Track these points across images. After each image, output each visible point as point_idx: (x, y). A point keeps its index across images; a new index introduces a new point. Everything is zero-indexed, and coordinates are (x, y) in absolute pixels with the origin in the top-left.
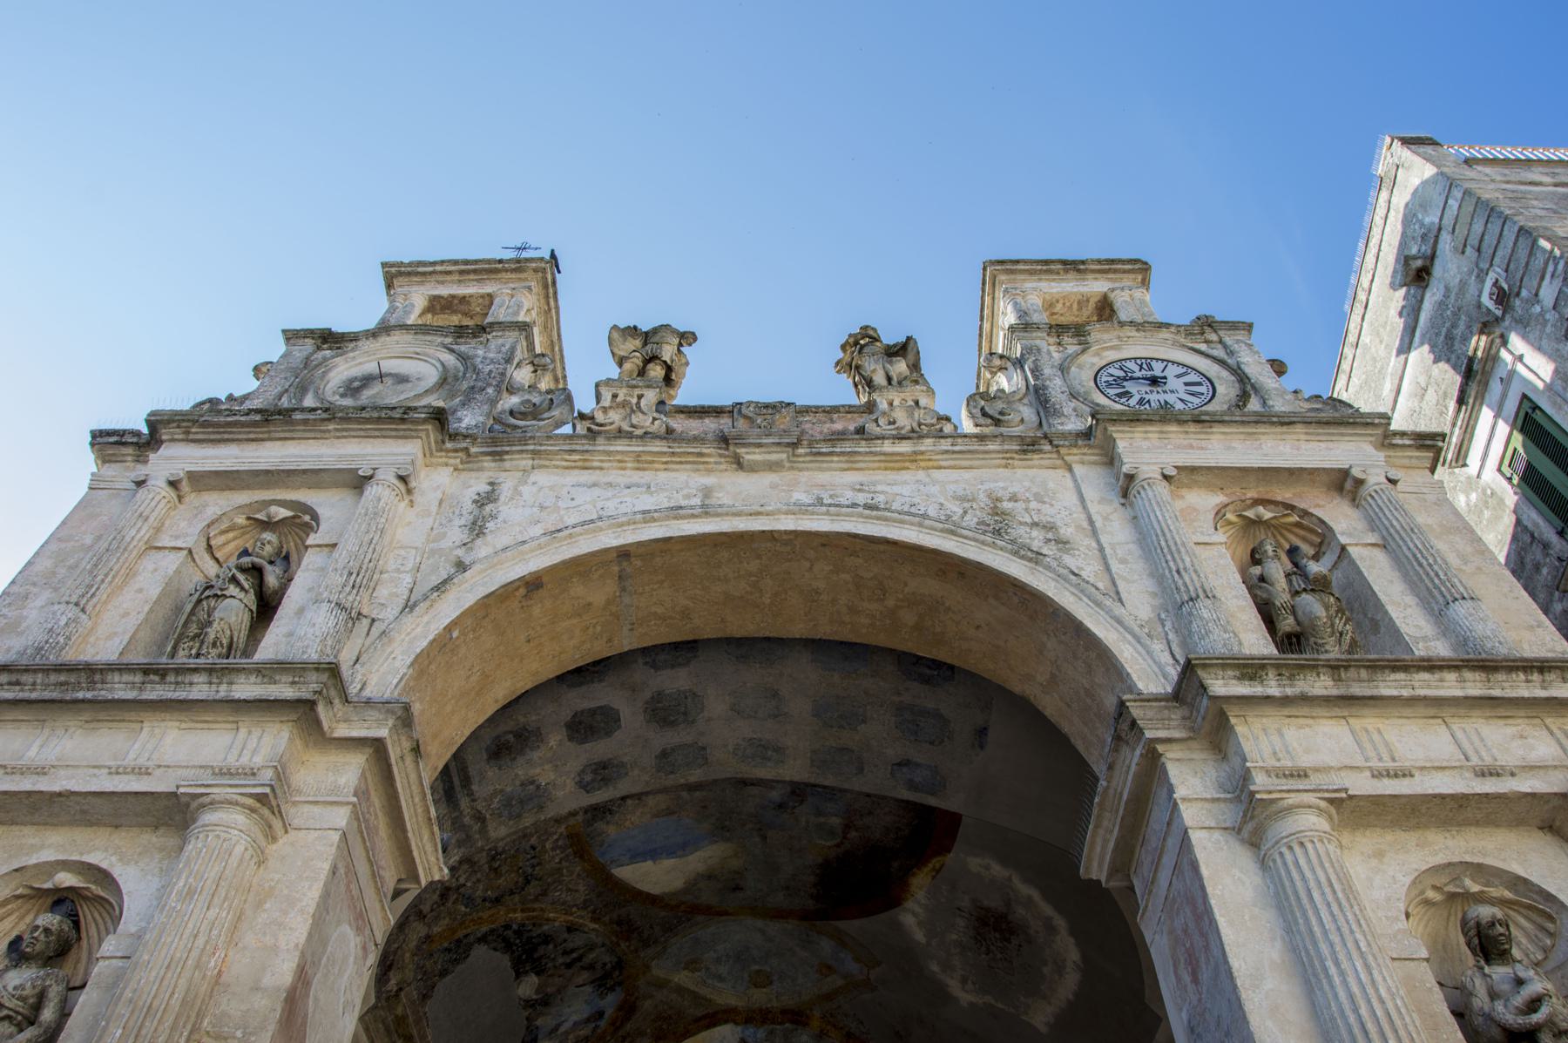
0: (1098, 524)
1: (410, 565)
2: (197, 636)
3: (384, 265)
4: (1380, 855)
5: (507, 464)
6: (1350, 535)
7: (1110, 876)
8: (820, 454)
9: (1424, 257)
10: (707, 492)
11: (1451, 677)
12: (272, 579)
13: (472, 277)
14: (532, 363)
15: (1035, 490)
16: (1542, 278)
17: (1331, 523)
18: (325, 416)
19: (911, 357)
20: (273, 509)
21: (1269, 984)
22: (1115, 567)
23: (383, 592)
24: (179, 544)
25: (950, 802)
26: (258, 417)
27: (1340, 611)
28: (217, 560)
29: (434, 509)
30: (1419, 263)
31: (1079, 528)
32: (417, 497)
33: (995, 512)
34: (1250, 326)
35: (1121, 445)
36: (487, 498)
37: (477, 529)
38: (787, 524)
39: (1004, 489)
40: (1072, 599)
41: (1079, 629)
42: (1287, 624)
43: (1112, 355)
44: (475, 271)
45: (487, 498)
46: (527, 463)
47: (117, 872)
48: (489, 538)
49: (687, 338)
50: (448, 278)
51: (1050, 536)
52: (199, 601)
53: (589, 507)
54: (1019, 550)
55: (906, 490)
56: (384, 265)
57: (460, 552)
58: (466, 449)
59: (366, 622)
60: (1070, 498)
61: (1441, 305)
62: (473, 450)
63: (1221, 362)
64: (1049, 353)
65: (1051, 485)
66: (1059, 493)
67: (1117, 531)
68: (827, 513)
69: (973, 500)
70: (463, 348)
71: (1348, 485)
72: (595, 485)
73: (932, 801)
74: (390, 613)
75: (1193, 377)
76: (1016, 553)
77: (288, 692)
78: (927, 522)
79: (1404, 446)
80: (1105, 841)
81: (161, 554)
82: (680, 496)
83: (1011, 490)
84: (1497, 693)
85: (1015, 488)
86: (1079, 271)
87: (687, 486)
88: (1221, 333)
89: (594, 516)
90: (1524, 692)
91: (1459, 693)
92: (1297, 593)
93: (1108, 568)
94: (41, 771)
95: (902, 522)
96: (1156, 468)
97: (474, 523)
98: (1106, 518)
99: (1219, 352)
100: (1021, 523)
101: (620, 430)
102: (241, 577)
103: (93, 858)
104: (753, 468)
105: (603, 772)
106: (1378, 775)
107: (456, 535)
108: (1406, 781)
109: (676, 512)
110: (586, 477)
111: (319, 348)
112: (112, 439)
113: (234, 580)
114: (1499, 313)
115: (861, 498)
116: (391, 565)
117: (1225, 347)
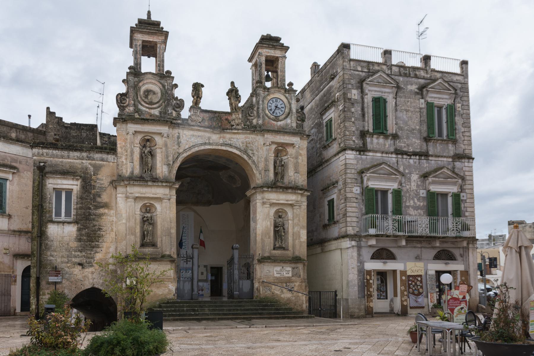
10: (209, 138)
30: (332, 77)
35: (266, 135)
36: (179, 137)
37: (179, 144)
43: (272, 96)
49: (203, 86)
54: (248, 156)
55: (235, 140)
63: (289, 102)
70: (162, 81)
72: (193, 136)
74: (171, 163)
75: (283, 106)
99: (289, 97)
103: (151, 202)
104: (215, 133)
109: (205, 144)
110: (191, 133)
115: (229, 142)
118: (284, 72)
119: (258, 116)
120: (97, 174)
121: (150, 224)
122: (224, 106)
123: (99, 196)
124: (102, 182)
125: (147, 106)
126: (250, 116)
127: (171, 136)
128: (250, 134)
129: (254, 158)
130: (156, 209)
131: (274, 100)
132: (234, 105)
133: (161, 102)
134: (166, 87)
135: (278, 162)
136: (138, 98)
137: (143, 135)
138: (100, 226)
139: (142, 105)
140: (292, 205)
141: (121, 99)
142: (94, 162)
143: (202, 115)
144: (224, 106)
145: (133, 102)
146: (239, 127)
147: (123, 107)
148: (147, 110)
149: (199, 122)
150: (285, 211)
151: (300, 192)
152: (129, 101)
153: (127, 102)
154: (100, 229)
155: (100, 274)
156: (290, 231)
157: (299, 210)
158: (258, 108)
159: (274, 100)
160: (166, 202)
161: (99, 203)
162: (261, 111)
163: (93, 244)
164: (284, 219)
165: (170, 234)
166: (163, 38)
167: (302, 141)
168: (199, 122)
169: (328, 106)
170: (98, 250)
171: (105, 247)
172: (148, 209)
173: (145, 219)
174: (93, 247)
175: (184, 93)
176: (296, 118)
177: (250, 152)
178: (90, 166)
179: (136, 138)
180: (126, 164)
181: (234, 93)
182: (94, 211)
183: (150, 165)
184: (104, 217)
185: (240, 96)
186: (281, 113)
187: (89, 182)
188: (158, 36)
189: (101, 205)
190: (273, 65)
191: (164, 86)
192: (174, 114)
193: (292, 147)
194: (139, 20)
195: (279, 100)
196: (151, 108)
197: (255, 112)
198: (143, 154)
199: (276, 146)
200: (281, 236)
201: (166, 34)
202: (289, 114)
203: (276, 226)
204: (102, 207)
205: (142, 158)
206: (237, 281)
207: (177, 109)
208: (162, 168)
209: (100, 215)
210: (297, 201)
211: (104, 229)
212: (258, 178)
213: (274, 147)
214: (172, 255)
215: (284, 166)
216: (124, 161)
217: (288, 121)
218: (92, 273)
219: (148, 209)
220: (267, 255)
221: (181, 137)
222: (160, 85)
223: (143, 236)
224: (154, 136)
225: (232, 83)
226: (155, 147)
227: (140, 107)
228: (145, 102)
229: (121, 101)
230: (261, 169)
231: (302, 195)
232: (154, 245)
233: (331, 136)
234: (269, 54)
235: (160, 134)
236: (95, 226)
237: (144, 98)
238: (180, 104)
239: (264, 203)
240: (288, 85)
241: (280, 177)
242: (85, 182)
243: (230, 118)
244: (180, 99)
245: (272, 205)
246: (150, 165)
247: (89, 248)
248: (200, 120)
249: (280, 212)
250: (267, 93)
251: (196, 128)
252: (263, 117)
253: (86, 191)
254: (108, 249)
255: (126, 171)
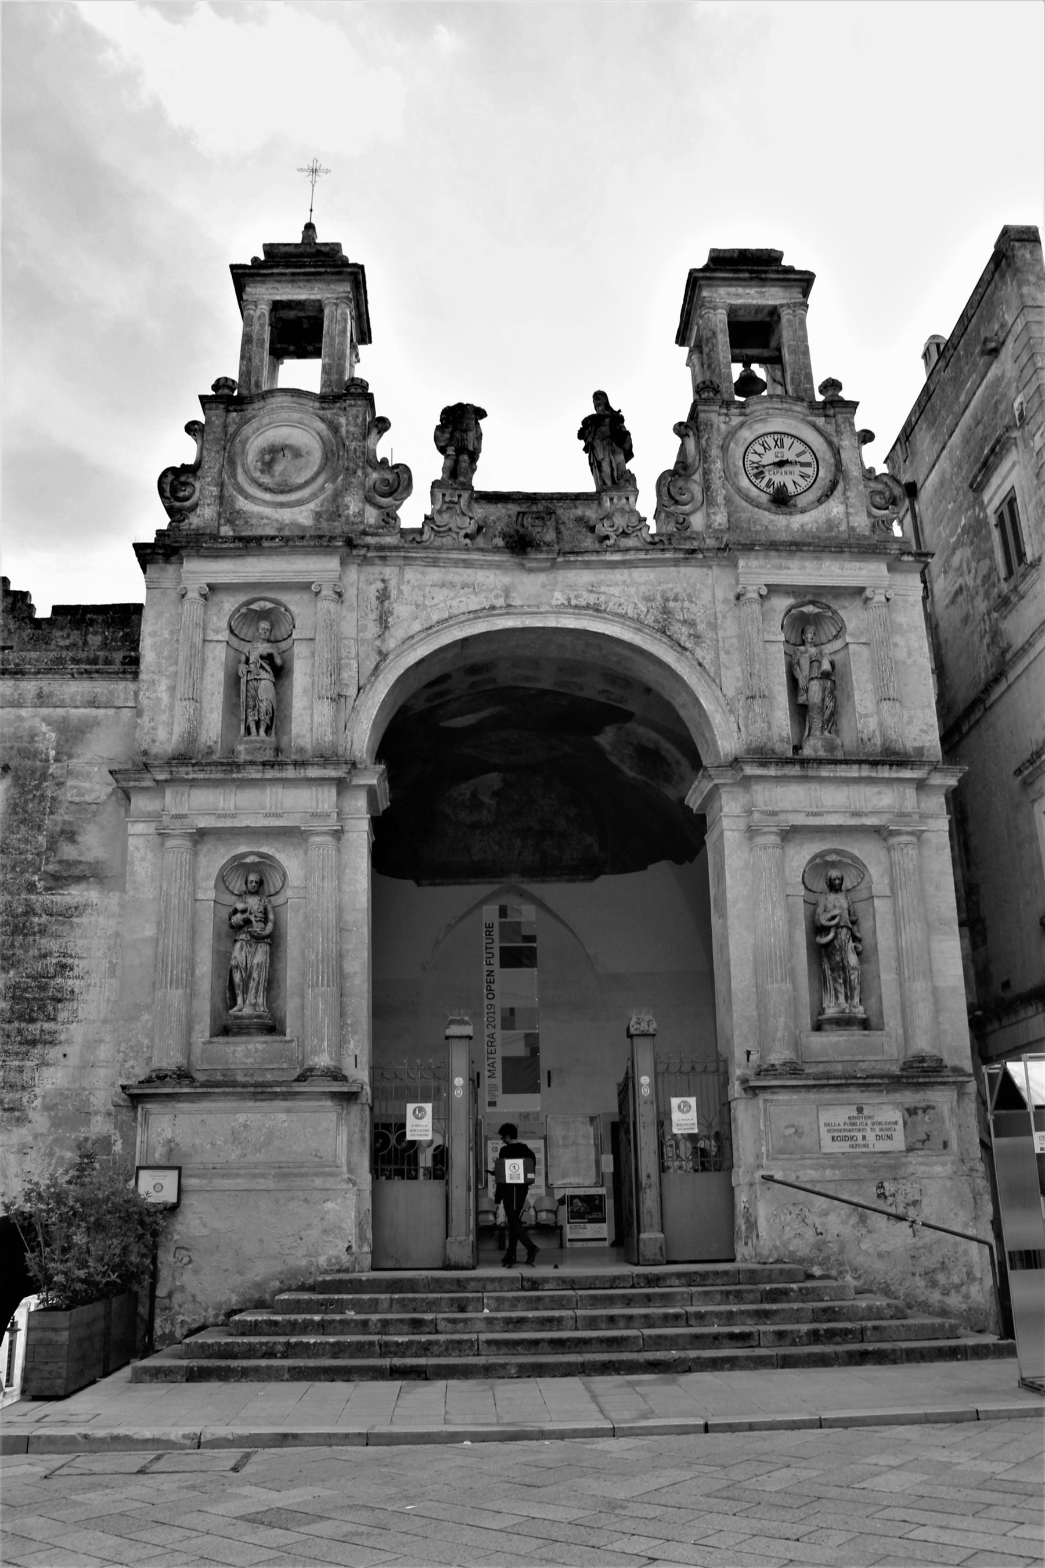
0: (719, 622)
1: (353, 654)
2: (255, 706)
3: (233, 267)
4: (801, 845)
5: (389, 563)
6: (852, 635)
7: (698, 809)
8: (570, 561)
9: (997, 341)
10: (507, 592)
11: (856, 767)
12: (278, 661)
13: (302, 278)
14: (377, 426)
15: (689, 591)
16: (1039, 429)
17: (846, 623)
18: (281, 543)
19: (626, 446)
20: (262, 604)
21: (740, 905)
22: (723, 656)
23: (345, 675)
24: (220, 637)
25: (630, 707)
26: (241, 545)
27: (832, 692)
28: (236, 635)
29: (355, 605)
30: (993, 345)
31: (709, 623)
32: (346, 596)
33: (666, 611)
34: (857, 403)
35: (741, 563)
36: (383, 596)
37: (383, 622)
38: (552, 622)
39: (672, 589)
40: (696, 681)
41: (697, 699)
42: (802, 699)
43: (760, 429)
44: (305, 274)
45: (383, 596)
46: (401, 562)
47: (277, 856)
48: (392, 630)
49: (481, 413)
50: (284, 278)
51: (692, 632)
52: (247, 681)
53: (442, 605)
55: (615, 591)
56: (233, 267)
57: (378, 643)
58: (365, 556)
59: (343, 700)
60: (706, 596)
61: (999, 380)
62: (369, 554)
63: (830, 443)
64: (718, 427)
65: (698, 585)
66: (702, 588)
67: (729, 629)
68: (574, 614)
69: (653, 600)
70: (328, 414)
71: (864, 596)
72: (443, 586)
73: (619, 705)
74: (352, 691)
75: (807, 458)
76: (672, 647)
77: (333, 774)
78: (627, 623)
79: (908, 562)
80: (696, 800)
81: (212, 645)
82: (491, 596)
83: (675, 591)
84: (874, 774)
85: (678, 589)
86: (762, 279)
87: (495, 587)
88: (837, 410)
89: (446, 615)
90: (886, 775)
91: (856, 775)
92: (812, 679)
93: (718, 656)
94: (233, 816)
95: (613, 621)
96: (755, 588)
97: (381, 617)
98: (724, 617)
99: (830, 429)
100: (678, 621)
101: (450, 529)
102: (265, 665)
103: (264, 849)
104: (531, 570)
105: (440, 695)
106: (808, 814)
107: (373, 629)
108: (819, 818)
110: (435, 574)
111: (228, 411)
112: (149, 551)
113: (262, 667)
114: (1018, 424)
115: (592, 599)
116: (344, 655)
117: (837, 425)
118: (806, 352)
119: (708, 498)
120: (70, 756)
121: (258, 939)
122: (572, 473)
123: (70, 835)
124: (87, 785)
125: (268, 497)
126: (677, 502)
127: (350, 594)
128: (676, 563)
129: (699, 653)
130: (285, 876)
131: (770, 441)
132: (606, 467)
133: (321, 480)
134: (343, 430)
135: (805, 663)
136: (234, 475)
137: (242, 598)
138: (65, 955)
139: (247, 496)
140: (880, 833)
141: (174, 484)
142: (60, 711)
143: (480, 511)
144: (572, 473)
145: (215, 490)
146: (630, 542)
147: (180, 510)
148: (267, 511)
149: (466, 536)
150: (854, 858)
151: (907, 774)
152: (204, 489)
153: (197, 494)
154: (64, 966)
155: (51, 1154)
156: (884, 941)
157: (913, 852)
158: (706, 473)
159: (770, 441)
160: (319, 846)
161: (69, 864)
162: (717, 482)
163: (34, 1029)
164: (855, 895)
165: (341, 976)
166: (345, 288)
167: (899, 579)
168: (466, 536)
169: (993, 450)
170: (53, 1053)
171: (78, 1039)
172: (253, 877)
173: (238, 918)
174: (34, 1043)
175: (411, 444)
176: (866, 501)
177: (682, 633)
178: (44, 728)
179: (213, 610)
180: (172, 707)
181: (605, 429)
182: (47, 898)
183: (264, 706)
184: (84, 920)
185: (628, 433)
186: (803, 484)
187: (37, 787)
188: (329, 282)
189: (76, 871)
190: (761, 336)
191: (334, 428)
192: (372, 516)
193: (858, 602)
194: (265, 245)
195: (787, 441)
196: (282, 505)
197: (697, 490)
198: (243, 668)
199: (790, 601)
200: (842, 968)
201: (356, 276)
202: (834, 485)
203: (817, 929)
204: (80, 879)
205: (234, 682)
206: (655, 1178)
207: (384, 501)
208: (312, 715)
209: (67, 914)
210: (902, 815)
211: (81, 966)
212: (725, 735)
213: (782, 604)
214: (349, 1070)
215: (832, 678)
216: (165, 697)
217: (835, 508)
218: (23, 1151)
219: (256, 877)
220: (779, 1056)
221: (394, 593)
222: (322, 426)
223: (230, 992)
224: (284, 597)
225: (600, 398)
226: (290, 641)
227: (242, 503)
228: (260, 485)
229: (174, 491)
230: (733, 698)
231: (921, 785)
232: (273, 1027)
233: (1021, 555)
234: (745, 314)
235: (306, 587)
236: (44, 956)
237: (258, 474)
238: (399, 481)
239: (752, 832)
240: (823, 389)
241: (816, 720)
242: (23, 786)
243: (591, 513)
244: (397, 466)
245: (790, 834)
246: (264, 706)
247: (16, 1048)
248: (471, 528)
249: (833, 865)
250: (736, 421)
251: (454, 555)
252: (728, 500)
253: (23, 822)
254: (90, 1052)
255: (165, 735)
